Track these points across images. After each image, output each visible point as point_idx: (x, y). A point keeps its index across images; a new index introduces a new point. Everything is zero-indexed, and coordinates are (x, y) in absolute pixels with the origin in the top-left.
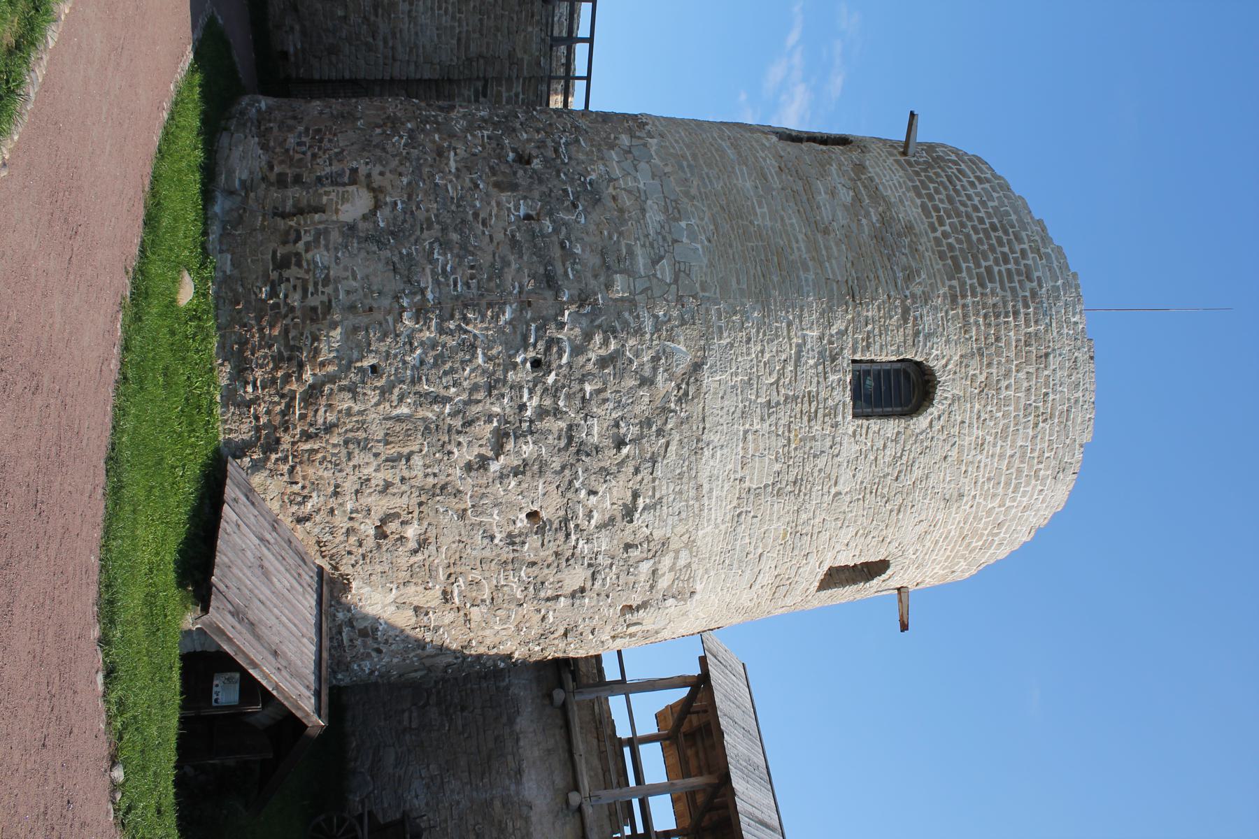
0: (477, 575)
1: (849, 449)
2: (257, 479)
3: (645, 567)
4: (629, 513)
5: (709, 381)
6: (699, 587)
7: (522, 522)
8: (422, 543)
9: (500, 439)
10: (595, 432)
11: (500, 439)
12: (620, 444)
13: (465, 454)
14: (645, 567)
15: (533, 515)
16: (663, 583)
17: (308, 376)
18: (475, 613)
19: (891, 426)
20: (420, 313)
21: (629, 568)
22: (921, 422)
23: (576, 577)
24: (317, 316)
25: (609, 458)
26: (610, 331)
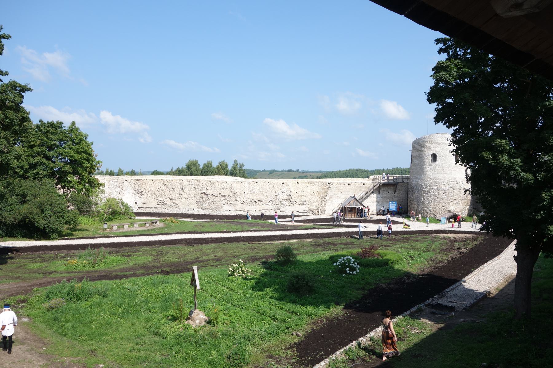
0: (449, 199)
1: (440, 163)
2: (438, 216)
3: (451, 182)
4: (444, 184)
5: (431, 177)
6: (454, 176)
7: (444, 194)
8: (445, 203)
9: (435, 196)
10: (435, 188)
11: (435, 196)
12: (437, 185)
13: (437, 199)
14: (451, 182)
15: (444, 193)
16: (453, 180)
17: (429, 211)
18: (454, 198)
19: (437, 158)
20: (424, 202)
21: (450, 184)
22: (437, 155)
23: (451, 189)
24: (424, 210)
25: (438, 186)
26: (426, 186)
